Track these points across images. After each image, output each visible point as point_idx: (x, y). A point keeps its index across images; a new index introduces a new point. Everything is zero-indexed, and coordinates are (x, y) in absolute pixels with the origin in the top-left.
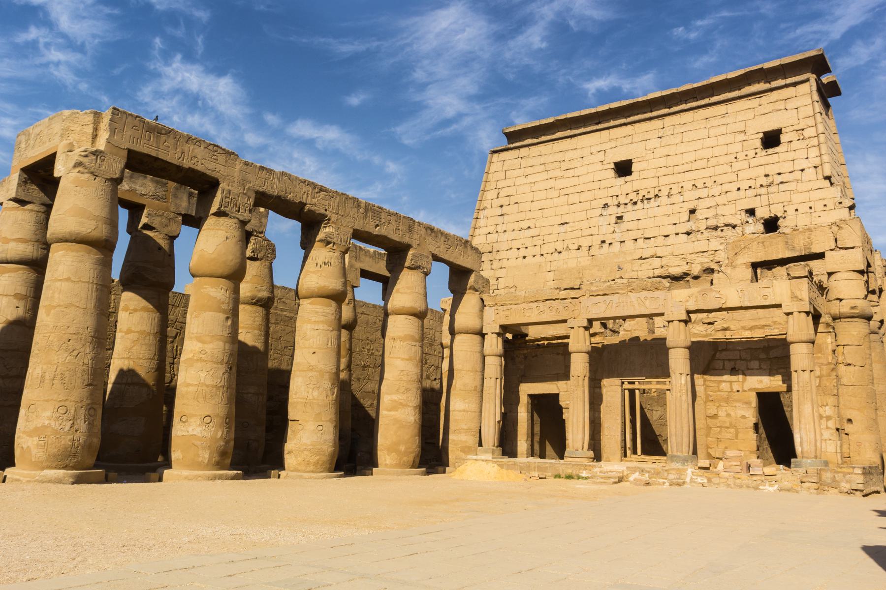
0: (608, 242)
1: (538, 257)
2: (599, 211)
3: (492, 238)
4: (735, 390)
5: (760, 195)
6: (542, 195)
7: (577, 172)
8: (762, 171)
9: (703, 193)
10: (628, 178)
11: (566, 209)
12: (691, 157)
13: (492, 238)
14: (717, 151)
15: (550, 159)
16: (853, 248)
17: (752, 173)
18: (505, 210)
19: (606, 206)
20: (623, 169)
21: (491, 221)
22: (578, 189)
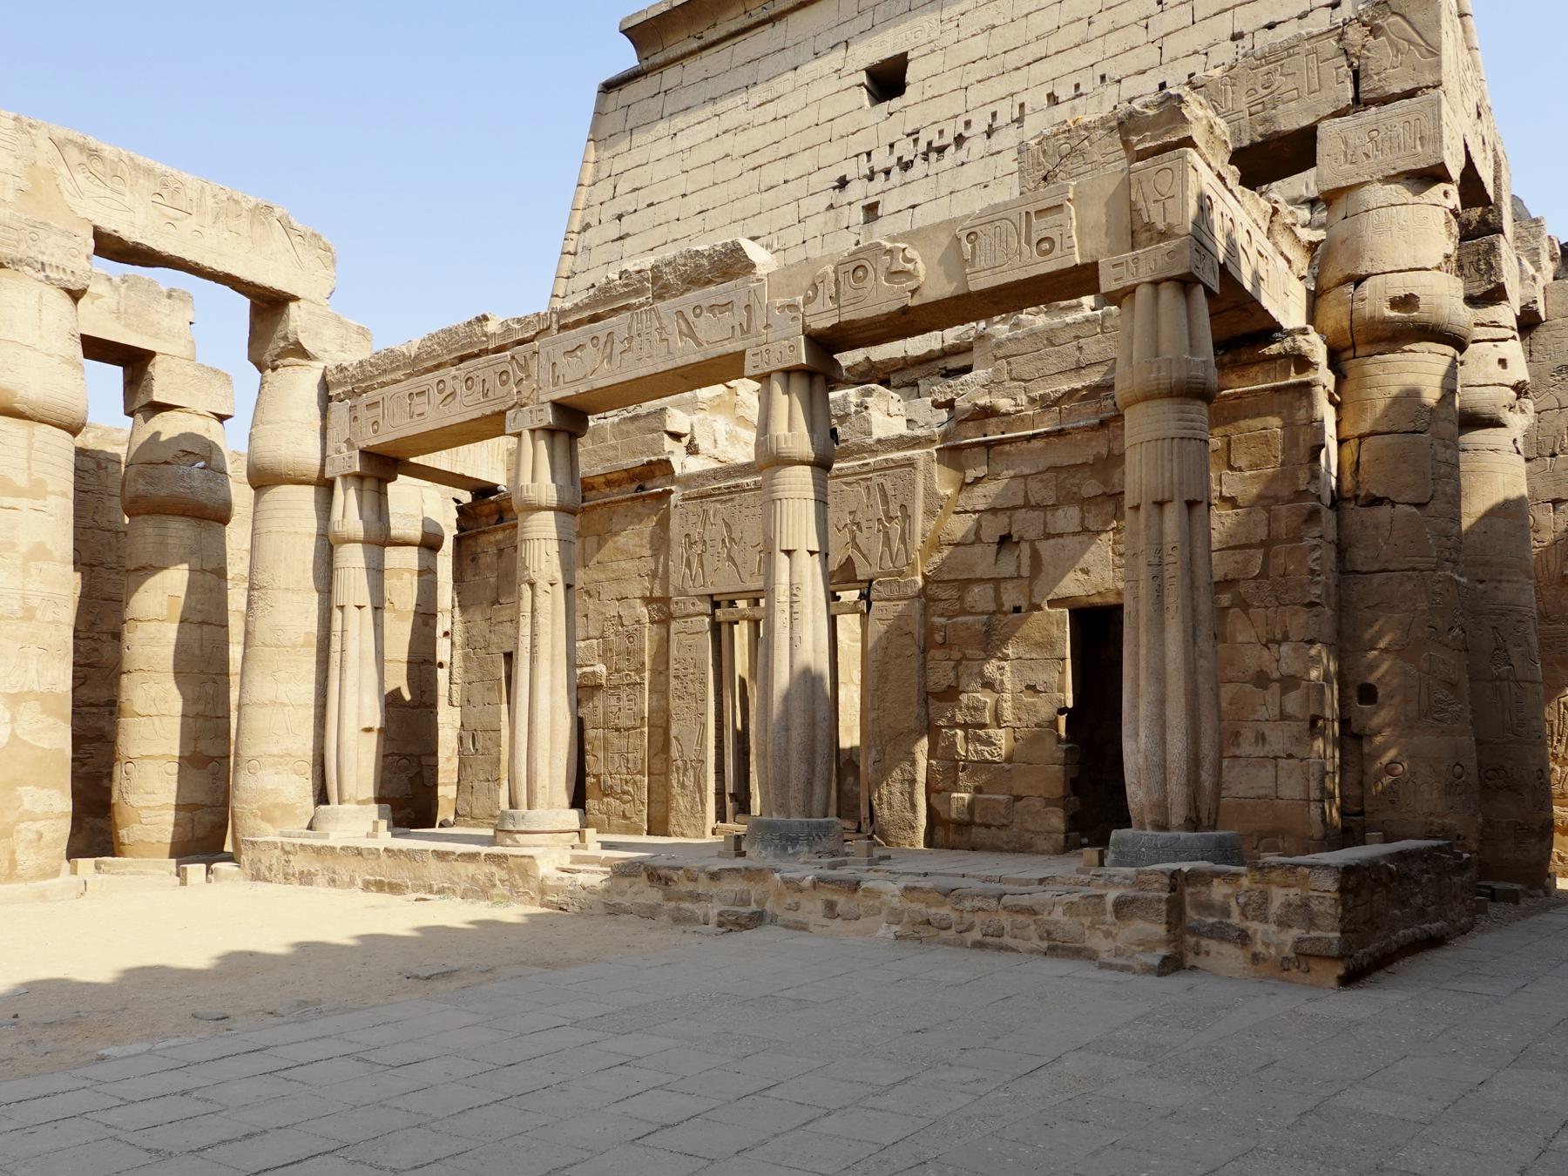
4: (1008, 606)
6: (706, 176)
10: (896, 103)
16: (1410, 94)
19: (843, 183)
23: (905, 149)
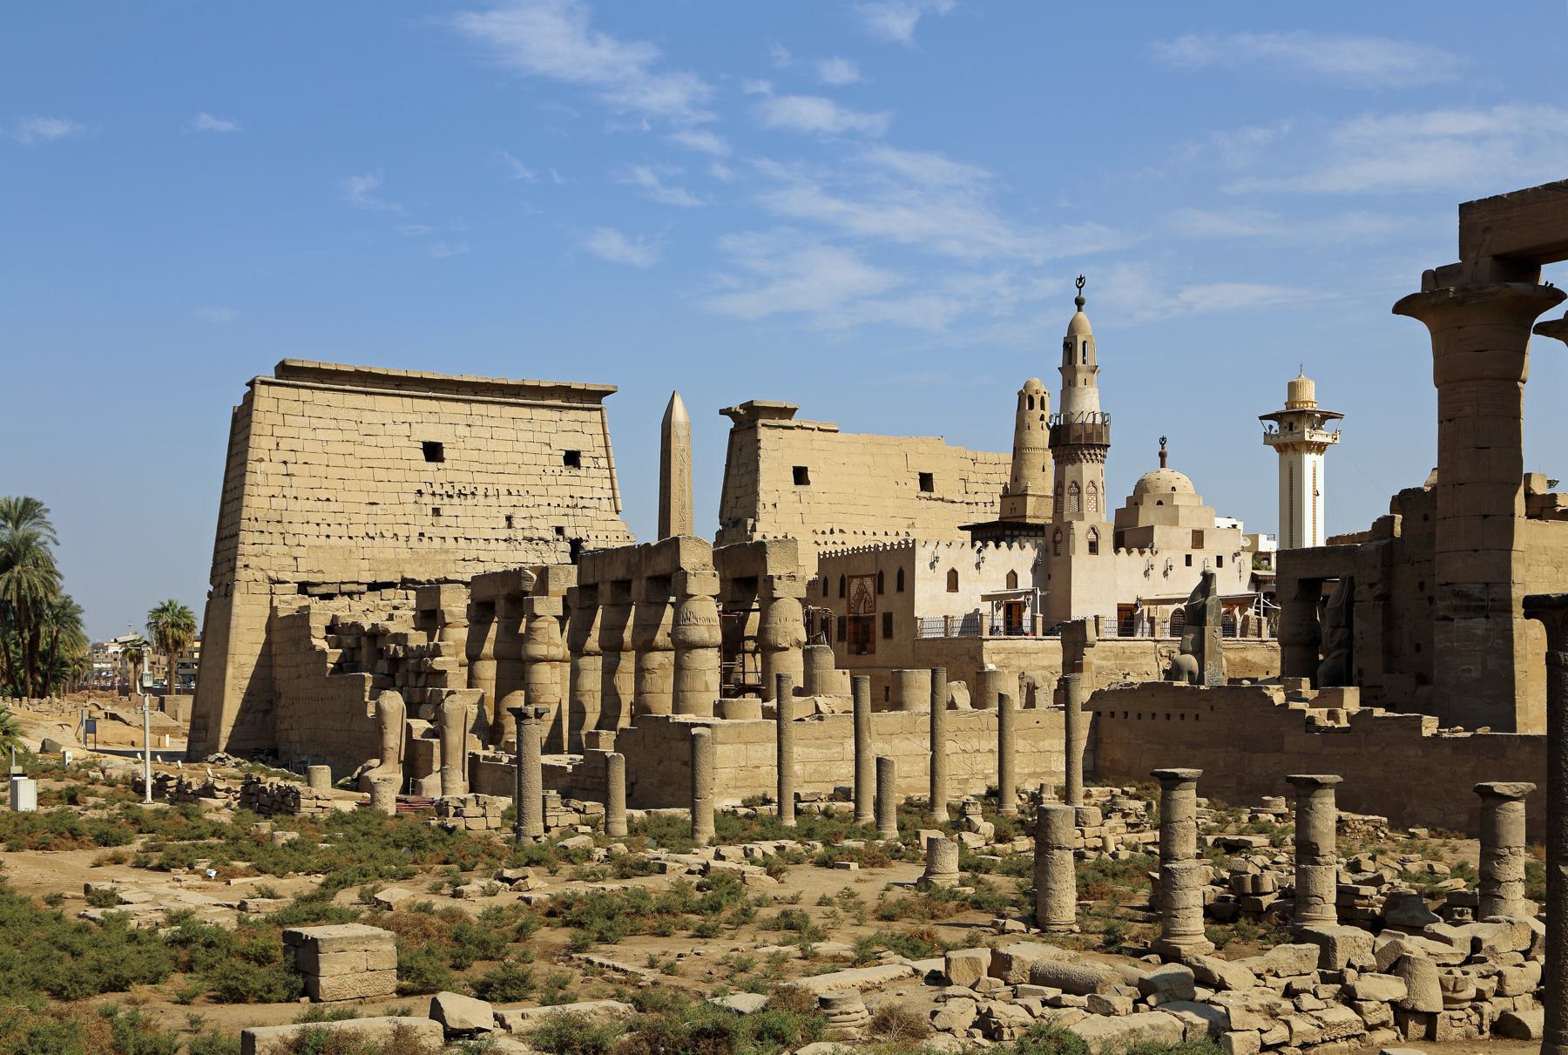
2: (412, 498)
3: (278, 503)
7: (381, 441)
8: (566, 491)
11: (372, 486)
12: (502, 458)
13: (278, 503)
14: (527, 458)
15: (342, 414)
18: (291, 468)
20: (433, 452)
21: (273, 480)
22: (384, 464)
23: (448, 487)
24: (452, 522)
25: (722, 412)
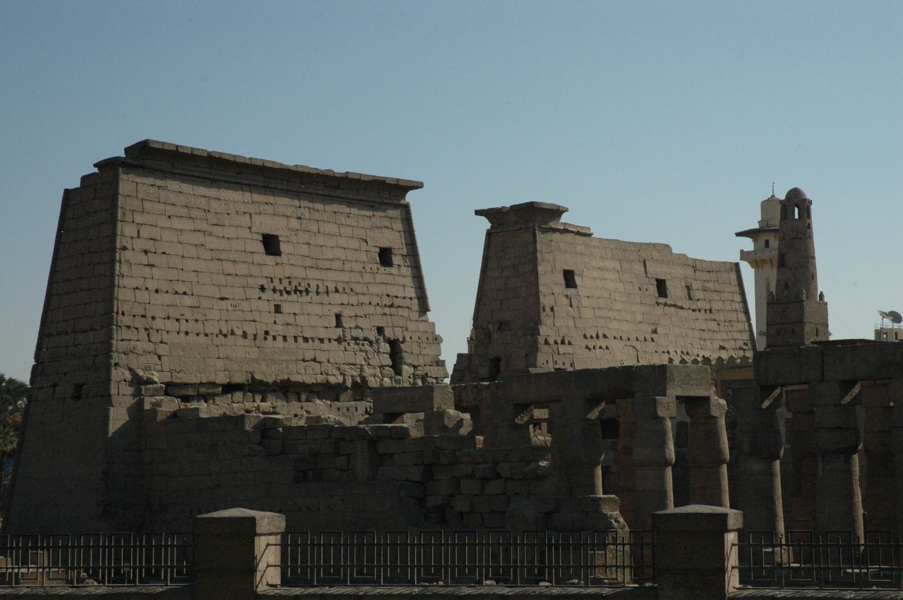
0: (272, 333)
1: (202, 336)
2: (256, 293)
5: (386, 314)
8: (383, 290)
9: (345, 299)
11: (222, 279)
13: (143, 296)
14: (350, 255)
17: (374, 289)
18: (152, 259)
22: (231, 257)
24: (291, 319)
25: (478, 213)
